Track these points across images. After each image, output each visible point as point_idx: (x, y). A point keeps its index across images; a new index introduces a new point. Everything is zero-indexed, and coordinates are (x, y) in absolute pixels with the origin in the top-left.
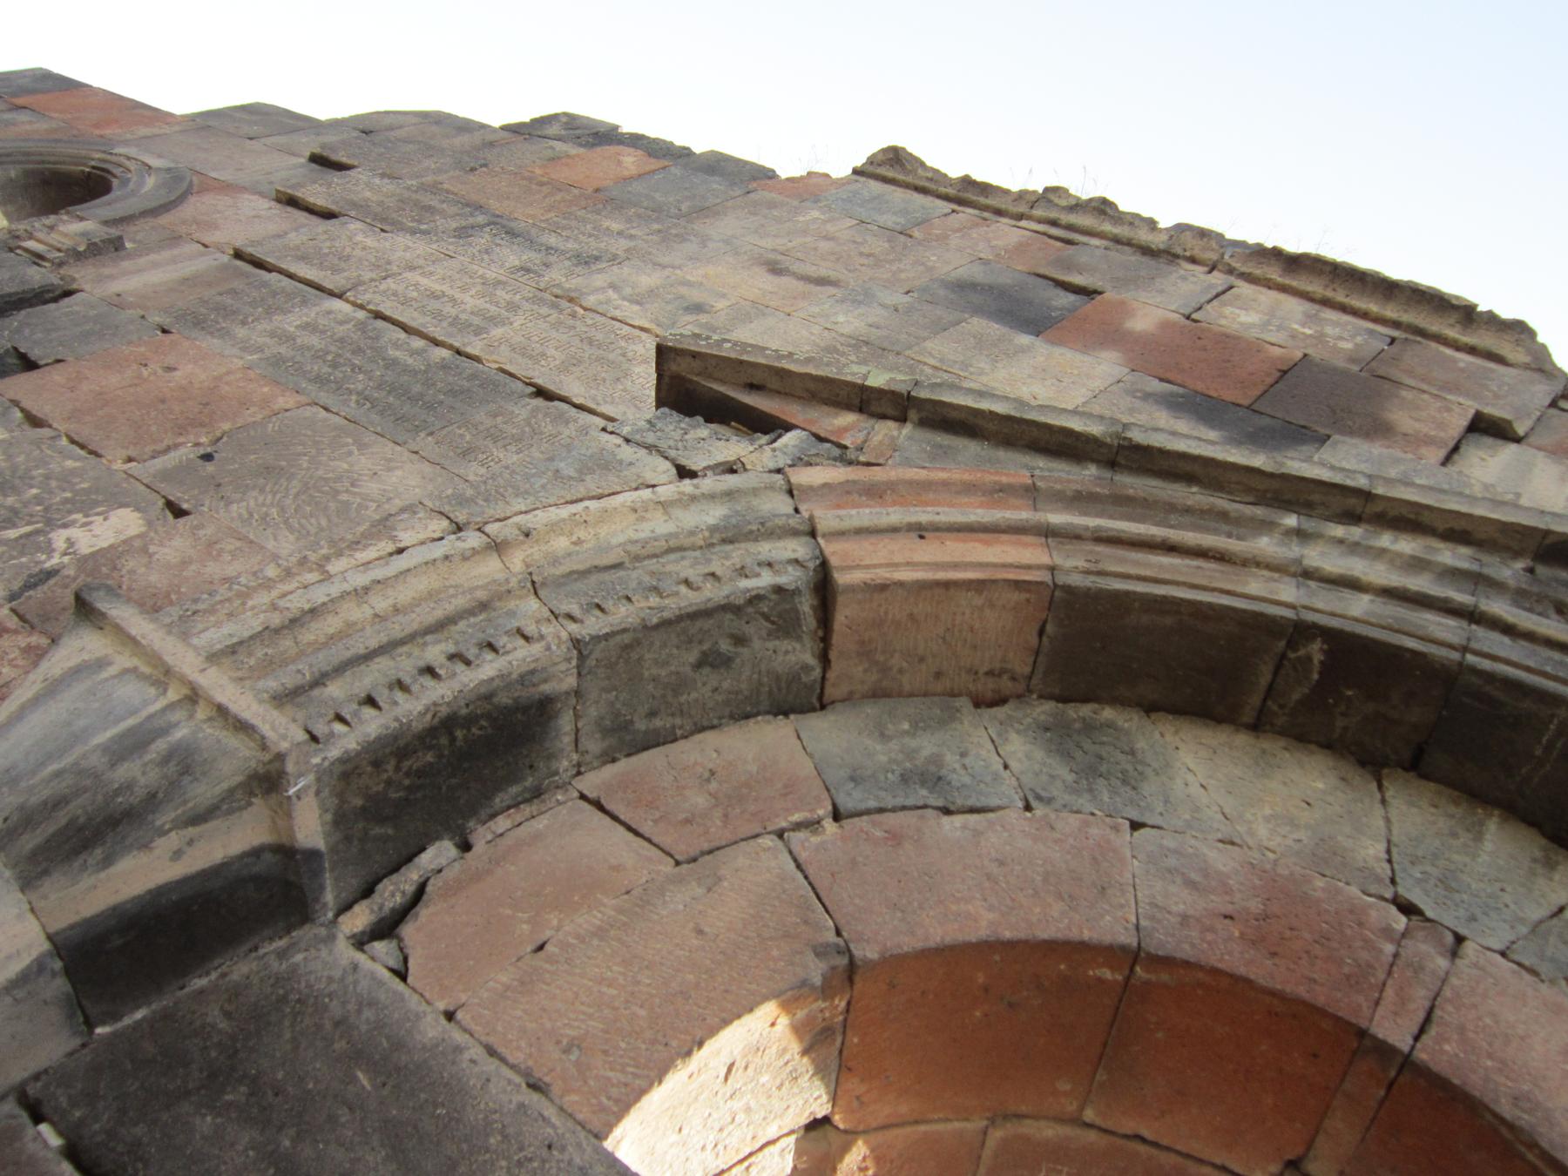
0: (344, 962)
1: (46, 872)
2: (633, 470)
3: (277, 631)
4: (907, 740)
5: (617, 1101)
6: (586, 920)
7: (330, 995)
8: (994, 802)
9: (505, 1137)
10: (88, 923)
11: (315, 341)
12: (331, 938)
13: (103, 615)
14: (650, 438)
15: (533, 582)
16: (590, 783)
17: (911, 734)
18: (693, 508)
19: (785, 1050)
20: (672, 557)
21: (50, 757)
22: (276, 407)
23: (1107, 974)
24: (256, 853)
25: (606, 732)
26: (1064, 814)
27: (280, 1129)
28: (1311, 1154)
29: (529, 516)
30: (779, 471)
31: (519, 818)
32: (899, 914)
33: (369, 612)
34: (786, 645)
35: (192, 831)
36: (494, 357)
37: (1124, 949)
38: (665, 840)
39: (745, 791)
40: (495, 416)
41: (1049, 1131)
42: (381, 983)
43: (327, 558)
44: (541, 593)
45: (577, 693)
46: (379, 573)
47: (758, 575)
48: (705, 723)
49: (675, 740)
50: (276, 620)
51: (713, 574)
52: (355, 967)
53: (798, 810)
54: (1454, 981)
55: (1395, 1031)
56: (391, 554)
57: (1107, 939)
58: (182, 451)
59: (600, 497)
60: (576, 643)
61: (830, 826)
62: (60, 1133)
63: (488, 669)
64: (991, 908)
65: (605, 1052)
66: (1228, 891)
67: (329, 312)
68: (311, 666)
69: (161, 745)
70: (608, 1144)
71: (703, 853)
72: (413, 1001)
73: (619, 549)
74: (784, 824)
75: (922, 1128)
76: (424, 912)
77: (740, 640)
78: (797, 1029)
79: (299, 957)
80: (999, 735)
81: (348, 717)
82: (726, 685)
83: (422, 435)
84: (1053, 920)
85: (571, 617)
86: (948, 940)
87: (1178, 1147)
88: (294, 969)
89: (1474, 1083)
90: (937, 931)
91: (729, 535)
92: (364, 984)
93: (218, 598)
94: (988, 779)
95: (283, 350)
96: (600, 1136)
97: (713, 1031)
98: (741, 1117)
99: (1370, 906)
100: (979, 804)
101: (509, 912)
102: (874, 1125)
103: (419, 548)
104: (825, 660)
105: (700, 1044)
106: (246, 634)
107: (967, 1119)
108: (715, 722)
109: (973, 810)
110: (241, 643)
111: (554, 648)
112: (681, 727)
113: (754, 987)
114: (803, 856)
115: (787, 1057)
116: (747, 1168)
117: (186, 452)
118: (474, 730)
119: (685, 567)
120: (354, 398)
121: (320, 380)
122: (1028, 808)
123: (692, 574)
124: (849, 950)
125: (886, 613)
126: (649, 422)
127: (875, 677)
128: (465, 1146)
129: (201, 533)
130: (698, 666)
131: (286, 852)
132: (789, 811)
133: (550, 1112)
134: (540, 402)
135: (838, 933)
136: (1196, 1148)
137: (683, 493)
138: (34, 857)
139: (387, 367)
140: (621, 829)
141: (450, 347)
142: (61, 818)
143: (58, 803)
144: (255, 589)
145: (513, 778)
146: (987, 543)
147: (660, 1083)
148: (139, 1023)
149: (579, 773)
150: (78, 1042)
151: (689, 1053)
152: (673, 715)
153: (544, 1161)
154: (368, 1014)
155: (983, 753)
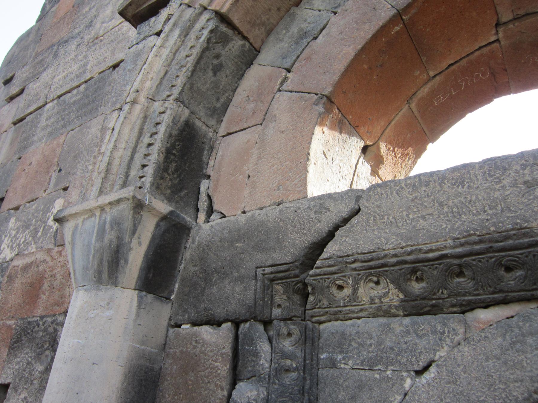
1: (116, 278)
2: (146, 48)
3: (106, 177)
4: (288, 34)
5: (301, 186)
6: (253, 159)
7: (213, 238)
8: (325, 22)
9: (283, 221)
10: (139, 277)
11: (53, 120)
12: (200, 227)
13: (64, 217)
14: (142, 36)
15: (151, 99)
16: (222, 131)
17: (288, 31)
18: (170, 38)
19: (334, 137)
20: (177, 55)
21: (88, 255)
22: (62, 143)
23: (397, 28)
24: (158, 225)
25: (212, 116)
26: (346, 3)
27: (232, 273)
28: (500, 16)
29: (134, 87)
30: (181, 5)
31: (214, 158)
32: (328, 73)
33: (122, 150)
34: (231, 45)
35: (136, 235)
36: (95, 73)
37: (394, 16)
38: (254, 122)
39: (260, 91)
40: (110, 85)
41: (426, 90)
42: (221, 223)
43: (99, 150)
44: (155, 99)
45: (193, 113)
46: (114, 139)
47: (203, 34)
48: (234, 88)
49: (231, 100)
50: (103, 175)
51: (192, 47)
52: (212, 226)
53: (277, 80)
56: (112, 132)
57: (387, 18)
58: (53, 176)
59: (145, 63)
60: (177, 100)
61: (289, 75)
62: (187, 324)
63: (162, 129)
64: (349, 46)
65: (288, 180)
67: (48, 110)
68: (121, 174)
69: (107, 226)
70: (310, 195)
71: (265, 115)
72: (232, 218)
73: (162, 68)
74: (278, 87)
75: (393, 123)
76: (214, 200)
77: (218, 56)
78: (332, 128)
79: (197, 238)
80: (310, 6)
81: (142, 175)
82: (228, 72)
83: (99, 109)
84: (369, 30)
85: (169, 96)
86: (346, 65)
87: (463, 56)
88: (199, 241)
90: (340, 66)
91: (185, 34)
92: (217, 228)
93: (85, 186)
94: (318, 18)
95: (48, 130)
96: (306, 197)
97: (309, 148)
98: (341, 165)
100: (322, 27)
101: (233, 178)
102: (379, 135)
103: (117, 123)
104: (245, 38)
105: (309, 154)
106: (100, 185)
107: (402, 109)
108: (236, 85)
109: (322, 31)
110: (101, 188)
111: (172, 107)
112: (229, 96)
113: (308, 128)
114: (290, 88)
115: (337, 138)
116: (358, 176)
117: (54, 175)
118: (177, 147)
119: (183, 53)
120: (75, 120)
121: (64, 126)
122: (335, 13)
123: (186, 53)
124: (324, 95)
125: (246, 7)
126: (138, 33)
127: (263, 29)
128: (276, 232)
129: (76, 185)
130: (215, 74)
131: (164, 218)
134: (117, 69)
135: (317, 94)
136: (468, 50)
137: (163, 38)
138: (110, 277)
139: (74, 105)
140: (240, 132)
141: (83, 83)
142: (106, 264)
143: (101, 261)
144: (91, 175)
145: (202, 150)
147: (308, 172)
148: (179, 288)
149: (217, 133)
150: (170, 304)
151: (308, 159)
152: (223, 94)
153: (298, 215)
154: (225, 232)
155: (311, 14)
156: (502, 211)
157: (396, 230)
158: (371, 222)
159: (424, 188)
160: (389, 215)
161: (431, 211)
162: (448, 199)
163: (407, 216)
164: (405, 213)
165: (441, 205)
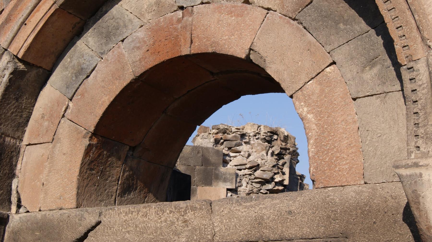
0: (18, 219)
6: (46, 172)
8: (95, 64)
12: (13, 217)
16: (26, 141)
17: (71, 62)
39: (51, 113)
42: (26, 216)
52: (20, 218)
53: (63, 107)
54: (194, 23)
55: (185, 51)
65: (66, 193)
66: (145, 42)
74: (63, 113)
88: (13, 227)
89: (203, 50)
90: (100, 112)
92: (24, 219)
99: (172, 16)
101: (34, 183)
132: (61, 109)
133: (64, 211)
146: (38, 11)
156: (159, 235)
157: (115, 237)
158: (106, 230)
159: (130, 215)
160: (114, 228)
161: (132, 229)
162: (140, 224)
163: (122, 230)
164: (121, 228)
165: (136, 226)
